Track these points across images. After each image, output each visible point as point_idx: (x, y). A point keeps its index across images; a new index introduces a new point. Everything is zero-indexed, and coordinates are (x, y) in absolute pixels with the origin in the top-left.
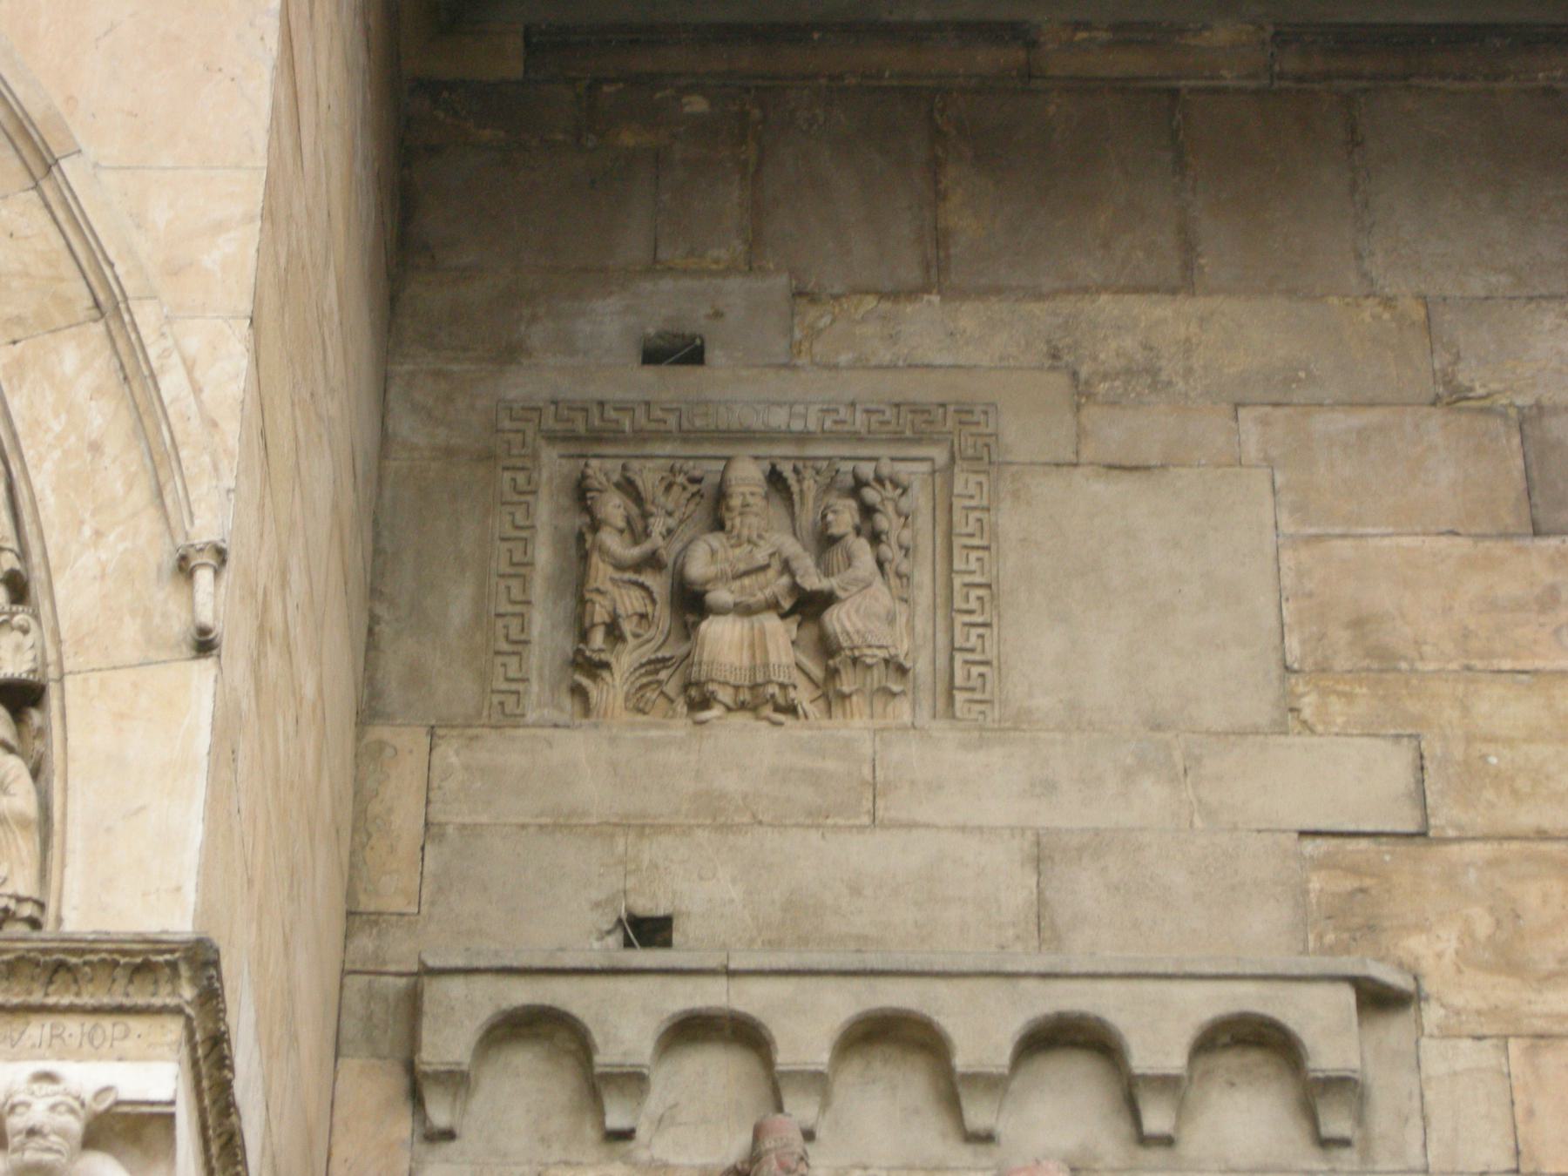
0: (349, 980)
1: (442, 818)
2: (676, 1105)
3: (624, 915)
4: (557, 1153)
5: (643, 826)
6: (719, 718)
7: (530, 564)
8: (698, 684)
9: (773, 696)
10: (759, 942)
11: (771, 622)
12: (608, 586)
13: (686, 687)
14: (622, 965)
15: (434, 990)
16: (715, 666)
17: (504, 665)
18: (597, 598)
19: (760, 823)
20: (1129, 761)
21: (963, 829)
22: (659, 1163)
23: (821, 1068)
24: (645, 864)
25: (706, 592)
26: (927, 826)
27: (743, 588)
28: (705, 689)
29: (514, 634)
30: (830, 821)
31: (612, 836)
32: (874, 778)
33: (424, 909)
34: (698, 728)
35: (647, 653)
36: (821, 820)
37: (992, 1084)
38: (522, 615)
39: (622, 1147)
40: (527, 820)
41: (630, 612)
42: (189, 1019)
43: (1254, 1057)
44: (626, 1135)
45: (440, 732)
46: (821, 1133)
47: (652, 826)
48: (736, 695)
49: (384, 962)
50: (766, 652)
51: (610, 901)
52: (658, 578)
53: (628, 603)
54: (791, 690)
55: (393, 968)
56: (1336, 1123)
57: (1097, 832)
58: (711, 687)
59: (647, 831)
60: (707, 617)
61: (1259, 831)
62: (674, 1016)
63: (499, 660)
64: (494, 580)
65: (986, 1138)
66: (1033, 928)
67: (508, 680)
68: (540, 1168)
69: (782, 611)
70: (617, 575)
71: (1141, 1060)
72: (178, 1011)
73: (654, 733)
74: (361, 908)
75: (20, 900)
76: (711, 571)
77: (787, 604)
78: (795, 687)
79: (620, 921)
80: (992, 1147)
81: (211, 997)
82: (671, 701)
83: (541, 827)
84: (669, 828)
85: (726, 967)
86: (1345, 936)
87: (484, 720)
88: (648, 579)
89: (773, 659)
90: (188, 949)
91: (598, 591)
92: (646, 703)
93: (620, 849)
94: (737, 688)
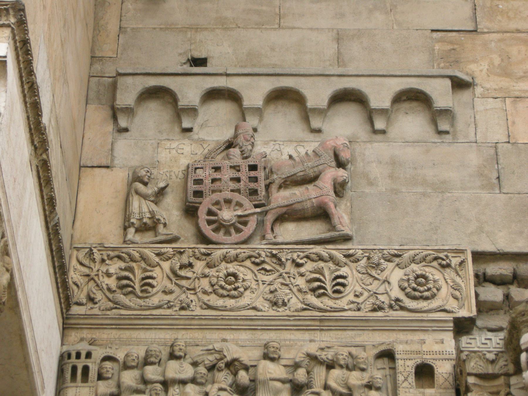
0: (91, 79)
1: (126, 26)
2: (207, 120)
3: (190, 58)
4: (165, 136)
5: (197, 28)
10: (238, 65)
14: (189, 72)
15: (121, 80)
19: (239, 27)
20: (371, 7)
21: (311, 29)
22: (201, 139)
23: (259, 106)
24: (198, 41)
26: (298, 28)
30: (264, 27)
31: (186, 32)
32: (280, 12)
33: (119, 56)
36: (261, 26)
37: (320, 112)
39: (188, 134)
40: (156, 26)
42: (13, 29)
43: (414, 104)
44: (190, 130)
46: (259, 130)
47: (200, 28)
49: (104, 73)
51: (185, 53)
55: (107, 75)
56: (444, 126)
57: (359, 30)
59: (199, 30)
61: (417, 30)
62: (207, 89)
65: (319, 131)
66: (336, 62)
68: (159, 141)
71: (374, 103)
72: (8, 26)
74: (96, 55)
79: (188, 60)
80: (321, 134)
81: (22, 23)
83: (161, 29)
84: (206, 29)
85: (226, 73)
86: (448, 64)
90: (13, 4)
93: (189, 36)
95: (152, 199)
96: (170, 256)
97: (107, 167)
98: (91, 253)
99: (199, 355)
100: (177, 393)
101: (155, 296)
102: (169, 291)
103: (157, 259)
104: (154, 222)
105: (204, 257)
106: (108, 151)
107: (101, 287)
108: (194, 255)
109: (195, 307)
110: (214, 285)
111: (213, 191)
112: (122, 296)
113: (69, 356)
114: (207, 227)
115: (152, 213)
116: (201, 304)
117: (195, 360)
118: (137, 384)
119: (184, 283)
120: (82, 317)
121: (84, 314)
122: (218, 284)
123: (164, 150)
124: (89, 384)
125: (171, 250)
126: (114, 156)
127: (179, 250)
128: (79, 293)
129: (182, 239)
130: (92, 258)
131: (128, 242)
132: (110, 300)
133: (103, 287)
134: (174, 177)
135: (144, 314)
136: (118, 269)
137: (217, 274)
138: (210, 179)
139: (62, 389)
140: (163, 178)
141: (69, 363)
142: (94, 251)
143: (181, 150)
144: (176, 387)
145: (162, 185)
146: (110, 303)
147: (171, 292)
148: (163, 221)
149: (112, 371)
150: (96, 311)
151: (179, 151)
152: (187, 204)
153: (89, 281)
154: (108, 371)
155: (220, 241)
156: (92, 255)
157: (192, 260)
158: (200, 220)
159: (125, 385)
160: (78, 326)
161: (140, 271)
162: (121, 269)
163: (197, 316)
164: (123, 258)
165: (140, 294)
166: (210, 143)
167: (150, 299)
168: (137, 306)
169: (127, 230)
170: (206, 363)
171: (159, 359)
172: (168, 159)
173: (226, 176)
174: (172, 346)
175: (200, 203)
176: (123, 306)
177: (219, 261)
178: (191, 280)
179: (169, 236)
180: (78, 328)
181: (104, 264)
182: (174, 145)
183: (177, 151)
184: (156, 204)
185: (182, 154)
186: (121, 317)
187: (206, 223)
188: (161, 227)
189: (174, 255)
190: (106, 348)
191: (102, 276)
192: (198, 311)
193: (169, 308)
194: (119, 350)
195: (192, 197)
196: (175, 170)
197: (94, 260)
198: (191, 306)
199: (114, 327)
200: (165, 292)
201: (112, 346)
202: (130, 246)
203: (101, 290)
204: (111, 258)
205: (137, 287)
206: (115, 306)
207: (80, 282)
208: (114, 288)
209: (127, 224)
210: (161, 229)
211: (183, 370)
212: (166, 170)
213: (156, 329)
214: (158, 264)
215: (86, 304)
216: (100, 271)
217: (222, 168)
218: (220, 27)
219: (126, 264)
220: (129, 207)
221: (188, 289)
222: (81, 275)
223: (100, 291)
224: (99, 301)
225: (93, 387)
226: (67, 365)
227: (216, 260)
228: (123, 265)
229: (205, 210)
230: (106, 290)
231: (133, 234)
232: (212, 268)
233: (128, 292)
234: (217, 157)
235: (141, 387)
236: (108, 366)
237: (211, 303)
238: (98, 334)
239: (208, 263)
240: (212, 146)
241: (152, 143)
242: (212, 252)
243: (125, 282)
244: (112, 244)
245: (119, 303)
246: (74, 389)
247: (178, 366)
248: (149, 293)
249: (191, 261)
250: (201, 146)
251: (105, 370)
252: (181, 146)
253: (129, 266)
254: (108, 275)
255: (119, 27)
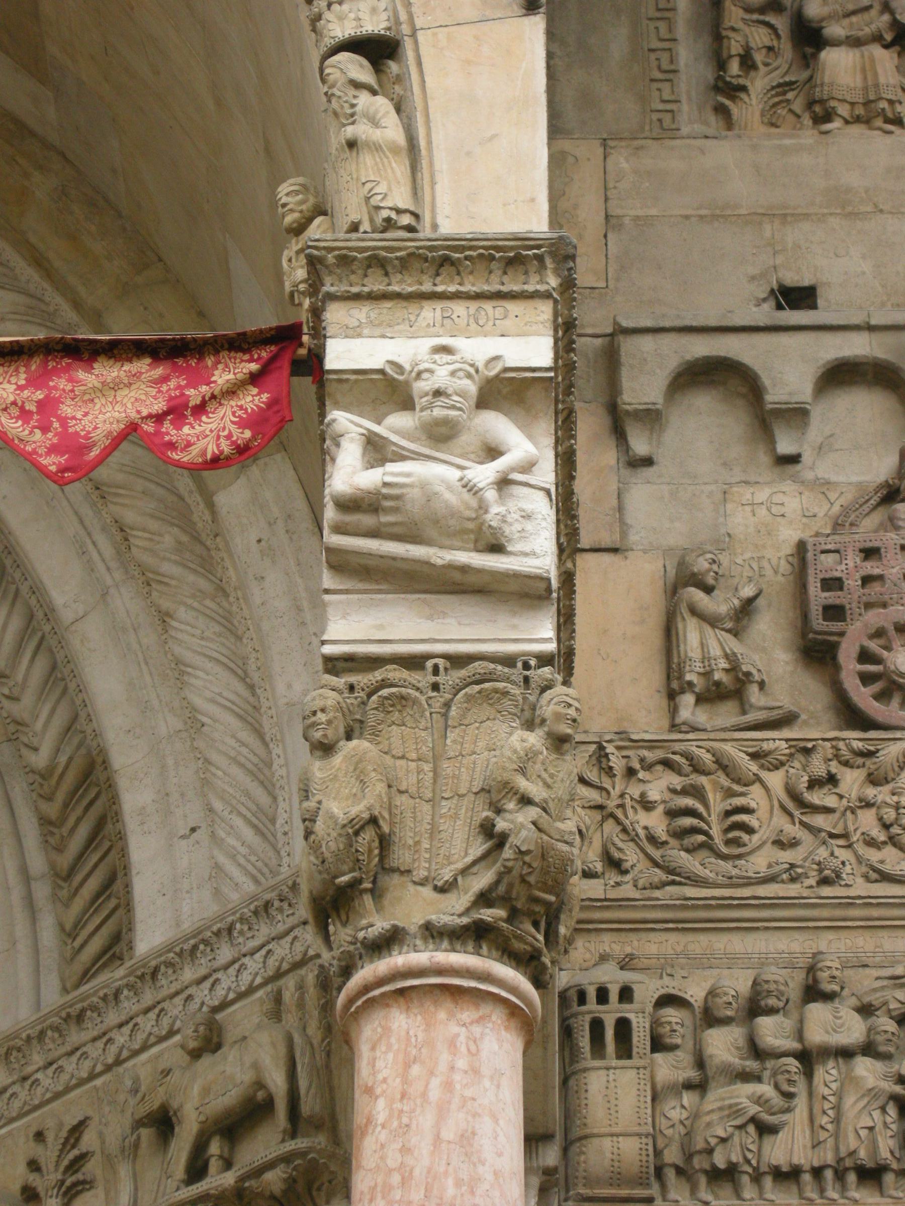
1: (619, 212)
2: (832, 435)
3: (775, 287)
4: (737, 475)
5: (785, 215)
6: (839, 129)
7: (673, 9)
8: (822, 102)
9: (883, 110)
10: (889, 304)
11: (877, 51)
12: (740, 25)
13: (810, 104)
15: (628, 346)
16: (835, 87)
17: (659, 90)
18: (731, 34)
19: (881, 211)
22: (822, 481)
24: (790, 245)
25: (822, 28)
27: (851, 24)
28: (828, 105)
29: (665, 66)
31: (760, 224)
33: (611, 284)
34: (823, 136)
35: (776, 78)
38: (670, 50)
41: (760, 46)
42: (556, 301)
44: (794, 459)
45: (611, 143)
47: (793, 215)
48: (852, 110)
50: (876, 75)
51: (763, 275)
52: (780, 18)
53: (757, 38)
54: (897, 105)
55: (590, 331)
58: (833, 103)
59: (789, 219)
60: (824, 48)
62: (828, 362)
63: (655, 85)
64: (645, 22)
67: (664, 101)
68: (725, 486)
69: (884, 43)
70: (747, 16)
72: (547, 295)
73: (787, 142)
75: (399, 211)
76: (825, 11)
77: (888, 37)
78: (900, 103)
82: (798, 116)
83: (701, 217)
84: (806, 216)
85: (868, 323)
87: (647, 134)
88: (771, 18)
89: (882, 80)
90: (552, 245)
91: (733, 29)
92: (778, 117)
93: (768, 233)
94: (852, 104)
95: (729, 625)
96: (783, 758)
97: (615, 550)
98: (601, 754)
99: (875, 990)
100: (833, 1078)
101: (757, 853)
102: (789, 842)
103: (754, 767)
104: (738, 679)
105: (860, 761)
106: (611, 513)
107: (634, 833)
108: (836, 757)
109: (852, 876)
110: (891, 825)
111: (868, 606)
112: (683, 853)
113: (582, 998)
114: (862, 689)
115: (731, 658)
116: (864, 869)
117: (866, 1000)
118: (741, 1059)
119: (819, 820)
120: (599, 904)
121: (603, 897)
122: (899, 823)
123: (740, 509)
124: (636, 1061)
125: (784, 745)
126: (627, 524)
127: (802, 744)
128: (584, 848)
129: (803, 717)
130: (604, 766)
131: (684, 728)
132: (656, 864)
133: (637, 835)
134: (769, 572)
135: (739, 896)
136: (665, 791)
137: (895, 798)
138: (858, 576)
139: (574, 1073)
140: (745, 574)
141: (583, 1014)
142: (608, 751)
143: (779, 507)
144: (831, 1063)
145: (748, 591)
146: (656, 870)
147: (794, 844)
148: (757, 677)
149: (681, 1030)
150: (627, 891)
151: (775, 510)
152: (811, 636)
153: (604, 820)
154: (675, 1031)
155: (894, 722)
156: (604, 760)
157: (834, 767)
158: (843, 675)
159: (717, 1061)
160: (590, 926)
161: (719, 796)
162: (674, 791)
163: (860, 897)
164: (676, 766)
165: (725, 850)
166: (844, 490)
167: (747, 861)
168: (720, 878)
169: (677, 699)
170: (891, 1007)
171: (784, 999)
172: (751, 530)
173: (894, 571)
174: (811, 969)
175: (842, 634)
176: (688, 878)
177: (897, 769)
178: (837, 815)
179: (776, 712)
180: (589, 931)
181: (633, 779)
182: (762, 495)
183: (769, 510)
184: (735, 635)
185: (783, 515)
186: (687, 904)
187: (858, 681)
188: (754, 689)
189: (791, 755)
190: (661, 977)
191: (632, 807)
192: (860, 888)
193: (793, 880)
194: (690, 979)
195: (821, 621)
196: (769, 553)
197: (609, 773)
198: (844, 876)
199: (671, 925)
200: (779, 844)
201: (673, 973)
202: (690, 736)
203: (633, 840)
204: (648, 767)
205: (716, 831)
206: (671, 877)
207: (585, 824)
208: (664, 837)
209: (675, 685)
210: (754, 695)
211: (842, 1026)
212: (748, 555)
213: (767, 928)
214: (758, 779)
215: (603, 874)
216: (627, 796)
217: (883, 550)
218: (838, 211)
219: (683, 778)
220: (678, 646)
221: (832, 836)
222: (583, 807)
223: (631, 844)
224: (633, 866)
225: (645, 1068)
226: (580, 1017)
227: (889, 767)
228: (677, 781)
229: (854, 651)
230: (645, 841)
231: (691, 709)
232: (881, 785)
233: (696, 845)
234: (864, 522)
235: (752, 1065)
236: (674, 1020)
237: (887, 868)
238: (636, 943)
239: (870, 775)
240: (848, 497)
241: (711, 492)
242: (879, 747)
243: (688, 821)
244: (647, 732)
245: (678, 870)
246: (603, 1073)
247: (831, 1017)
248: (745, 845)
249: (833, 771)
250: (821, 496)
251: (668, 1028)
252: (778, 498)
253: (691, 785)
254: (647, 805)
255: (603, 214)
